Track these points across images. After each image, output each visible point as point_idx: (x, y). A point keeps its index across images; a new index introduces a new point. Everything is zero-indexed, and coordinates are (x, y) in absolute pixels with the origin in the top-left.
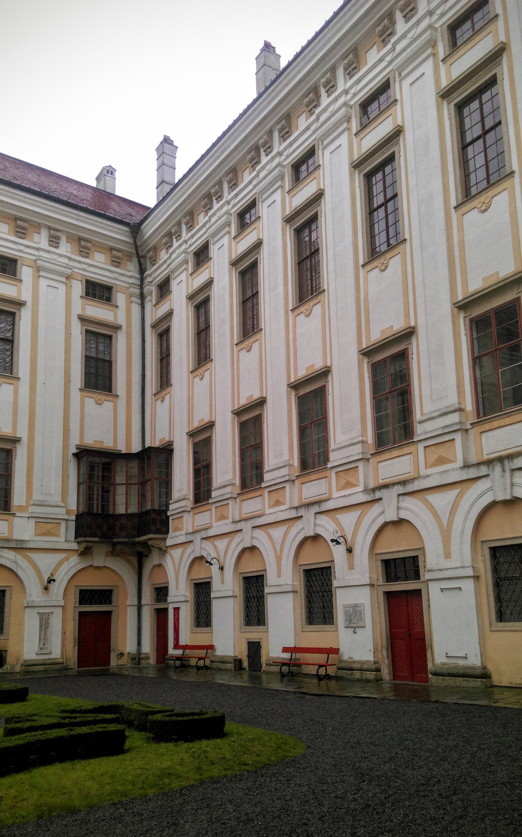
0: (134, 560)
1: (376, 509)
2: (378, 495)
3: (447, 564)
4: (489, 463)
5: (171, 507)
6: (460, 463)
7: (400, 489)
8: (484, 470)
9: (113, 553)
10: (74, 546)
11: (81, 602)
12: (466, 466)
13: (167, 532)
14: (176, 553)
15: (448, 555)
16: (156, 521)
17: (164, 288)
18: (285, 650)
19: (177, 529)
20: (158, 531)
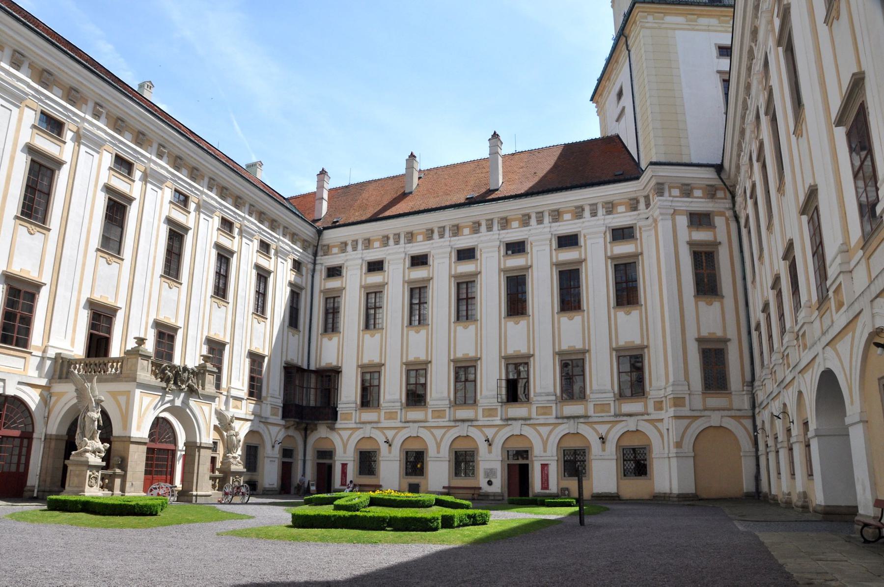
0: (303, 432)
1: (507, 429)
2: (510, 422)
3: (545, 454)
4: (568, 418)
5: (339, 406)
6: (554, 416)
7: (523, 422)
8: (565, 421)
9: (296, 429)
10: (283, 422)
11: (318, 458)
12: (557, 418)
13: (336, 419)
14: (345, 434)
15: (545, 451)
16: (327, 412)
17: (334, 272)
18: (444, 487)
19: (346, 419)
20: (332, 419)
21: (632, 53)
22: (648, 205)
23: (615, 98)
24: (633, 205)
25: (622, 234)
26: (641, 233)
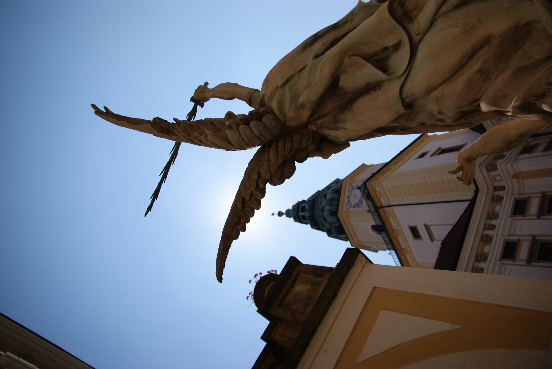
21: (392, 203)
22: (502, 188)
23: (418, 242)
24: (498, 200)
25: (520, 208)
26: (524, 194)
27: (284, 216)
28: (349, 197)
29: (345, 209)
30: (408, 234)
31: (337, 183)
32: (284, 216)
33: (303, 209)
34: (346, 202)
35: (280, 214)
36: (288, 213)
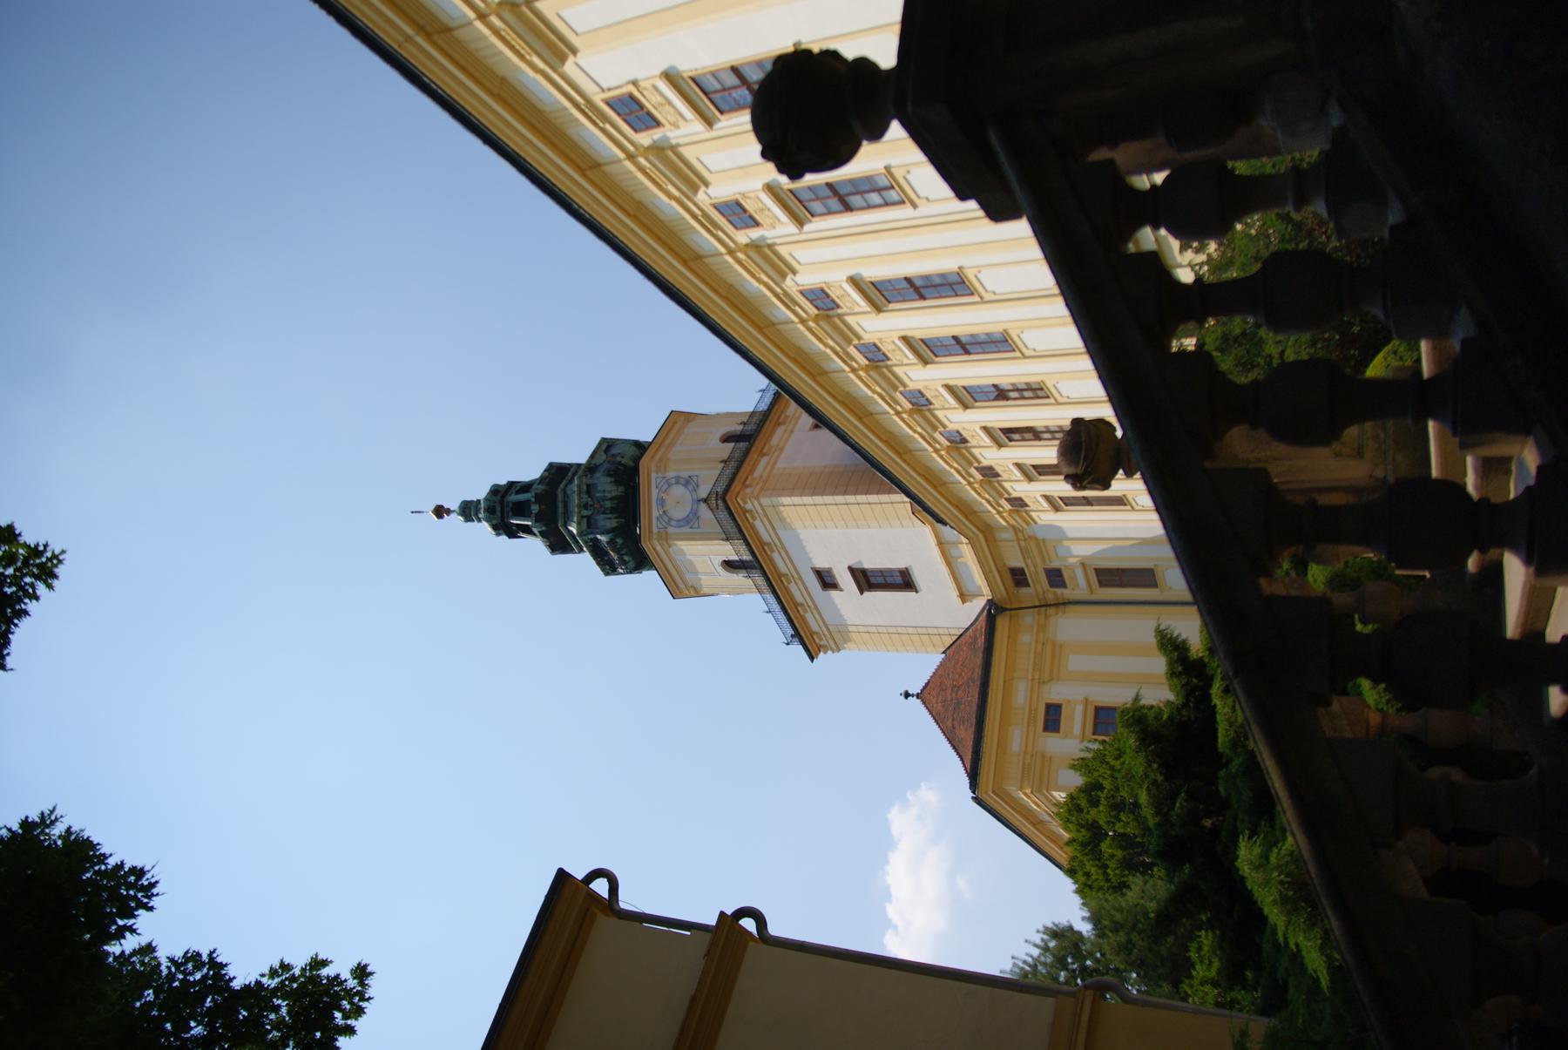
27: (453, 516)
28: (662, 502)
29: (655, 530)
30: (813, 583)
31: (606, 451)
32: (456, 520)
33: (521, 509)
34: (655, 514)
35: (440, 512)
36: (468, 510)
